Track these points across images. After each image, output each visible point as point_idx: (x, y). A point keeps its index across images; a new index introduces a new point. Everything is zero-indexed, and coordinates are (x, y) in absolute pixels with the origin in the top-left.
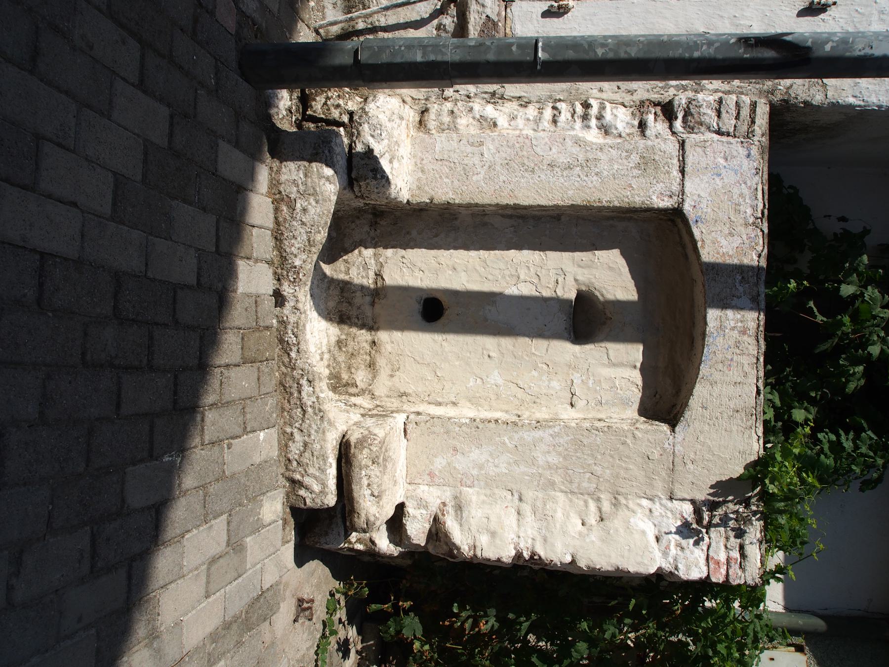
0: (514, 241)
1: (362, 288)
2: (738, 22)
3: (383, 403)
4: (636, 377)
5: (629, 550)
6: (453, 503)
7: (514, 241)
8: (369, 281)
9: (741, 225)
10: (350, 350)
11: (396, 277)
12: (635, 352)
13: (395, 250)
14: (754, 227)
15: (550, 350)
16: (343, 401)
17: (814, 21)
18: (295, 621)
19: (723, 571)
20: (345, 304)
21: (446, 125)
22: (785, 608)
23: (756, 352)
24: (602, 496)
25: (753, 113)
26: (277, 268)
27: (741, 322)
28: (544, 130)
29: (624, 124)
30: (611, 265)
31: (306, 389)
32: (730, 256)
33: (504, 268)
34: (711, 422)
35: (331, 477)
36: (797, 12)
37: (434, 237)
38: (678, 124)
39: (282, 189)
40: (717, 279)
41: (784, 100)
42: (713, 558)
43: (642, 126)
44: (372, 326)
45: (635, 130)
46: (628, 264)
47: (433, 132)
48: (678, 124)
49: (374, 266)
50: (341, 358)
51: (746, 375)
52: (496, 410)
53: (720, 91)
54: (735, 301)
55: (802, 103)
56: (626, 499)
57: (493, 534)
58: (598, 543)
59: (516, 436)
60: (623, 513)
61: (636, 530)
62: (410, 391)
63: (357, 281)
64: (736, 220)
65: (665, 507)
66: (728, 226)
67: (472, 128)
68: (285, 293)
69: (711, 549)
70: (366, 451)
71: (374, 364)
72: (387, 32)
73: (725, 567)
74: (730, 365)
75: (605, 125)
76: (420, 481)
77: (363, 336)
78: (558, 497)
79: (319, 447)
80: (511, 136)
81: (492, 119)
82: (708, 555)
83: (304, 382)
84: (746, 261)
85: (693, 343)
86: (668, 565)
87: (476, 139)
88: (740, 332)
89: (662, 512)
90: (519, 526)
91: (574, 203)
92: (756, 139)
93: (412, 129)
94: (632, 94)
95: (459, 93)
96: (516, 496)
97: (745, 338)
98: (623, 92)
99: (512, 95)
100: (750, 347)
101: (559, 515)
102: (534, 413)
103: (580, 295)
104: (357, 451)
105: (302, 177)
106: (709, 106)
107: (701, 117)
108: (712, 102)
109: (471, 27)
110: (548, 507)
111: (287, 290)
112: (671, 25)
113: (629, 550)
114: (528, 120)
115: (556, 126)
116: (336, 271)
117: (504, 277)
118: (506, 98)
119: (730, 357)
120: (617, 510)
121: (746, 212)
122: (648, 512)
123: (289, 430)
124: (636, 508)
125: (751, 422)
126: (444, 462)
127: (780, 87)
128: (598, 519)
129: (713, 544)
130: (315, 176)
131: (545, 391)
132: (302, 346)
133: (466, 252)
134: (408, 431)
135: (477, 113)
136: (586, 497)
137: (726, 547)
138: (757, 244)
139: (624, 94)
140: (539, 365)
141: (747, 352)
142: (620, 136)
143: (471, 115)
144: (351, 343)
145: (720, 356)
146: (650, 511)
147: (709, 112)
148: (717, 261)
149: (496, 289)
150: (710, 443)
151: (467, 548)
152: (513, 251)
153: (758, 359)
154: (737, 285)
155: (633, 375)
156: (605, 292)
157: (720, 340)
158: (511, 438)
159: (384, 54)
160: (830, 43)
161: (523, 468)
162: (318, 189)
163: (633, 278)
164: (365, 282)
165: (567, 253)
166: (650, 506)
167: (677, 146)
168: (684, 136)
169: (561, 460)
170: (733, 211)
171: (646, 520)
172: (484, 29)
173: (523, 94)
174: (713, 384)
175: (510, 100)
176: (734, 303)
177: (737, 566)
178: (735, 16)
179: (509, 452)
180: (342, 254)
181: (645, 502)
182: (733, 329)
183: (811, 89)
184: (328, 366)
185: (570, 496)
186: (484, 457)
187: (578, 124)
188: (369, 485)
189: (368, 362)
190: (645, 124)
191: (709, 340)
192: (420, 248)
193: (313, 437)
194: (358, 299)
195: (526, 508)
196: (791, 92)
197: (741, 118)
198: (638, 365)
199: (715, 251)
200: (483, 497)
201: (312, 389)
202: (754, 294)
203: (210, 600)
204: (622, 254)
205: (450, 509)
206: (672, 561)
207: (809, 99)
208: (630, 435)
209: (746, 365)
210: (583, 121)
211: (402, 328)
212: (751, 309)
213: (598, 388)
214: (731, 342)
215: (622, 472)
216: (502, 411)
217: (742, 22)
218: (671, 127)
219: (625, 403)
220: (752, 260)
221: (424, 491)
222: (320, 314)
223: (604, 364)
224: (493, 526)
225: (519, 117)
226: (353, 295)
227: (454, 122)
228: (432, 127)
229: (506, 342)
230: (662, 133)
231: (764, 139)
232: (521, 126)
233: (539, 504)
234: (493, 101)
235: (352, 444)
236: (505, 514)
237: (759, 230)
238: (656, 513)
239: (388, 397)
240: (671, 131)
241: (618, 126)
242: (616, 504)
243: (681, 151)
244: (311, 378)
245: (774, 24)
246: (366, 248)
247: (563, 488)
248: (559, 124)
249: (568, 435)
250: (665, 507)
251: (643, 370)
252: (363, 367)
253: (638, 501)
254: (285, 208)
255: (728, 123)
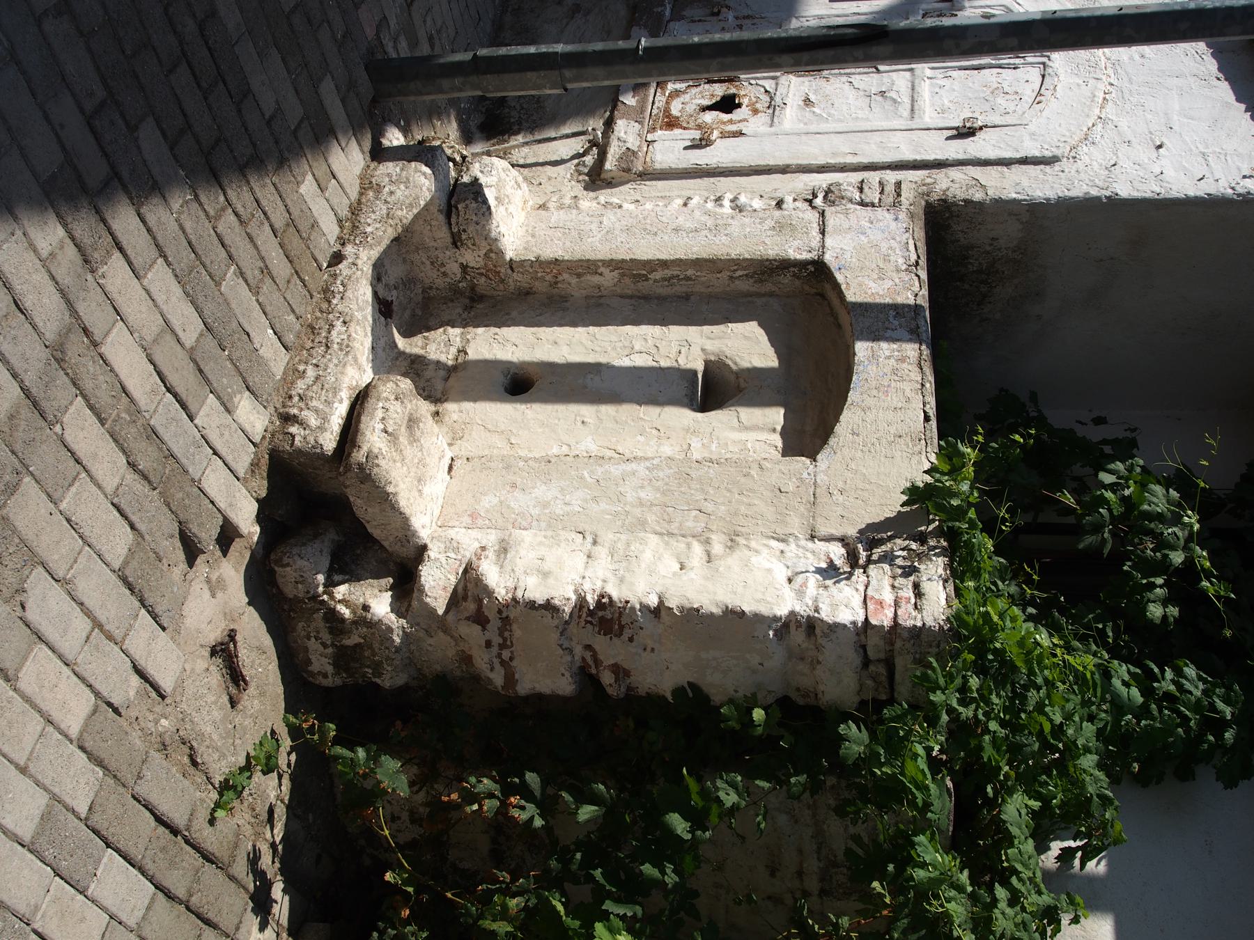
19: (889, 613)
23: (920, 379)
24: (713, 537)
35: (337, 413)
42: (872, 598)
51: (908, 400)
54: (889, 333)
56: (747, 539)
57: (546, 575)
65: (804, 548)
69: (870, 588)
73: (893, 610)
84: (900, 300)
88: (897, 360)
96: (589, 539)
97: (905, 365)
101: (648, 555)
104: (379, 383)
113: (745, 587)
116: (411, 345)
117: (614, 348)
119: (886, 384)
122: (778, 553)
126: (495, 501)
129: (873, 582)
133: (572, 329)
134: (455, 468)
136: (690, 539)
137: (893, 587)
148: (865, 300)
149: (603, 359)
151: (503, 592)
153: (923, 385)
154: (891, 319)
156: (738, 360)
158: (592, 473)
161: (603, 506)
163: (772, 346)
164: (443, 358)
166: (782, 548)
176: (887, 335)
177: (911, 608)
182: (889, 358)
185: (666, 538)
188: (383, 419)
197: (886, 193)
198: (779, 428)
204: (760, 325)
206: (810, 603)
212: (910, 340)
214: (888, 370)
229: (607, 410)
238: (788, 554)
242: (732, 545)
244: (347, 319)
247: (658, 528)
251: (784, 433)
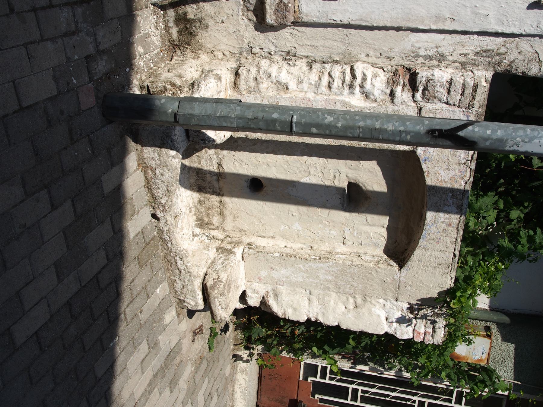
0: (306, 151)
1: (210, 172)
2: (478, 11)
3: (231, 235)
4: (385, 233)
5: (369, 324)
6: (273, 292)
7: (306, 151)
8: (215, 169)
9: (456, 164)
10: (207, 206)
11: (231, 167)
12: (385, 220)
13: (228, 151)
14: (465, 166)
15: (330, 214)
16: (207, 234)
17: (541, 13)
18: (193, 341)
19: (422, 337)
20: (200, 181)
21: (252, 88)
22: (490, 307)
23: (456, 236)
24: (357, 296)
25: (475, 92)
26: (152, 203)
27: (449, 219)
28: (322, 94)
29: (380, 92)
30: (370, 170)
31: (179, 262)
32: (446, 182)
33: (300, 167)
34: (423, 269)
35: (199, 299)
36: (527, 5)
37: (253, 145)
38: (419, 95)
39: (146, 161)
40: (435, 195)
41: (507, 70)
42: (417, 331)
43: (392, 94)
44: (219, 193)
45: (388, 98)
46: (381, 170)
47: (244, 93)
48: (419, 95)
49: (216, 159)
50: (203, 210)
51: (448, 247)
52: (298, 243)
53: (458, 62)
54: (446, 208)
55: (521, 73)
56: (371, 298)
57: (295, 309)
58: (353, 319)
59: (307, 265)
60: (368, 305)
61: (375, 314)
62: (246, 229)
63: (206, 168)
64: (452, 161)
65: (393, 304)
66: (446, 164)
67: (271, 90)
68: (159, 216)
69: (416, 327)
70: (216, 291)
71: (223, 213)
72: (206, 2)
73: (423, 335)
74: (438, 241)
75: (366, 92)
76: (254, 281)
77: (215, 199)
78: (332, 294)
79: (190, 287)
80: (298, 99)
81: (285, 84)
82: (414, 329)
83: (177, 258)
84: (456, 186)
85: (422, 217)
86: (391, 331)
87: (273, 99)
88: (447, 225)
89: (391, 306)
90: (309, 306)
91: (342, 144)
92: (474, 109)
93: (229, 89)
94: (390, 60)
95: (264, 50)
96: (308, 292)
97: (450, 228)
98: (384, 58)
99: (302, 54)
100: (452, 233)
101: (332, 303)
102: (320, 246)
103: (350, 184)
104: (211, 291)
105: (157, 156)
106: (442, 85)
107: (435, 93)
108: (445, 83)
109: (267, 7)
110: (326, 299)
111: (160, 214)
112: (424, 11)
113: (369, 324)
114: (311, 84)
115: (330, 90)
116: (192, 162)
117: (300, 172)
118: (298, 56)
119: (439, 237)
120: (365, 303)
121: (460, 156)
122: (383, 305)
123: (173, 278)
124: (375, 303)
125: (448, 270)
126: (266, 274)
127: (505, 61)
128: (354, 306)
129: (418, 325)
130: (165, 156)
131: (327, 235)
132: (174, 242)
133: (275, 155)
134: (245, 258)
135: (274, 78)
136: (348, 295)
137: (425, 326)
138: (465, 176)
139: (385, 60)
140: (323, 222)
141: (450, 236)
142: (376, 101)
143: (270, 80)
144: (207, 202)
145: (432, 236)
146: (384, 305)
147: (441, 90)
148: (437, 185)
149: (295, 179)
150: (421, 278)
151: (281, 314)
152: (305, 157)
153: (456, 240)
154: (449, 199)
155: (382, 231)
156: (366, 185)
157: (434, 228)
158: (304, 266)
159: (193, 120)
160: (490, 140)
161: (311, 280)
162: (168, 164)
163: (384, 178)
164: (211, 169)
165: (341, 161)
166: (384, 303)
167: (416, 110)
168: (422, 104)
169: (333, 278)
170: (452, 155)
171: (381, 309)
172: (278, 9)
173: (310, 54)
174: (427, 250)
175: (301, 58)
176: (445, 209)
177: (430, 336)
178: (476, 6)
179: (303, 272)
180: (195, 152)
181: (381, 301)
182: (443, 223)
183: (529, 64)
184: (195, 214)
185: (338, 294)
186: (289, 273)
187: (347, 90)
188: (220, 304)
189: (219, 212)
190: (394, 95)
191: (426, 227)
192: (244, 151)
193: (187, 283)
194: (208, 178)
195: (314, 298)
196: (513, 64)
197: (465, 95)
198: (386, 226)
199: (436, 179)
200: (289, 291)
201: (182, 262)
202: (459, 204)
203: (145, 374)
204: (378, 164)
205: (271, 294)
206: (393, 330)
207: (526, 71)
208: (374, 270)
209: (449, 242)
210: (350, 89)
211: (238, 196)
212: (456, 213)
213: (360, 237)
214: (441, 230)
215: (369, 287)
216: (301, 243)
217: (480, 12)
218: (413, 96)
219: (376, 246)
220: (461, 185)
221: (256, 285)
222: (185, 188)
223: (364, 224)
224: (294, 305)
225: (304, 82)
226: (205, 176)
227: (257, 86)
228: (243, 89)
229: (303, 209)
230: (406, 100)
231: (480, 110)
232: (306, 89)
233: (321, 297)
234: (288, 57)
235: (208, 287)
236: (302, 300)
237: (468, 168)
238: (387, 307)
239: (233, 231)
240: (413, 99)
241: (375, 94)
242: (365, 300)
243: (418, 114)
244: (181, 257)
245: (507, 14)
246: (210, 149)
247: (335, 290)
248: (332, 90)
249: (337, 267)
250: (393, 304)
251: (388, 229)
252: (216, 215)
253: (377, 300)
254: (150, 172)
255: (456, 97)
